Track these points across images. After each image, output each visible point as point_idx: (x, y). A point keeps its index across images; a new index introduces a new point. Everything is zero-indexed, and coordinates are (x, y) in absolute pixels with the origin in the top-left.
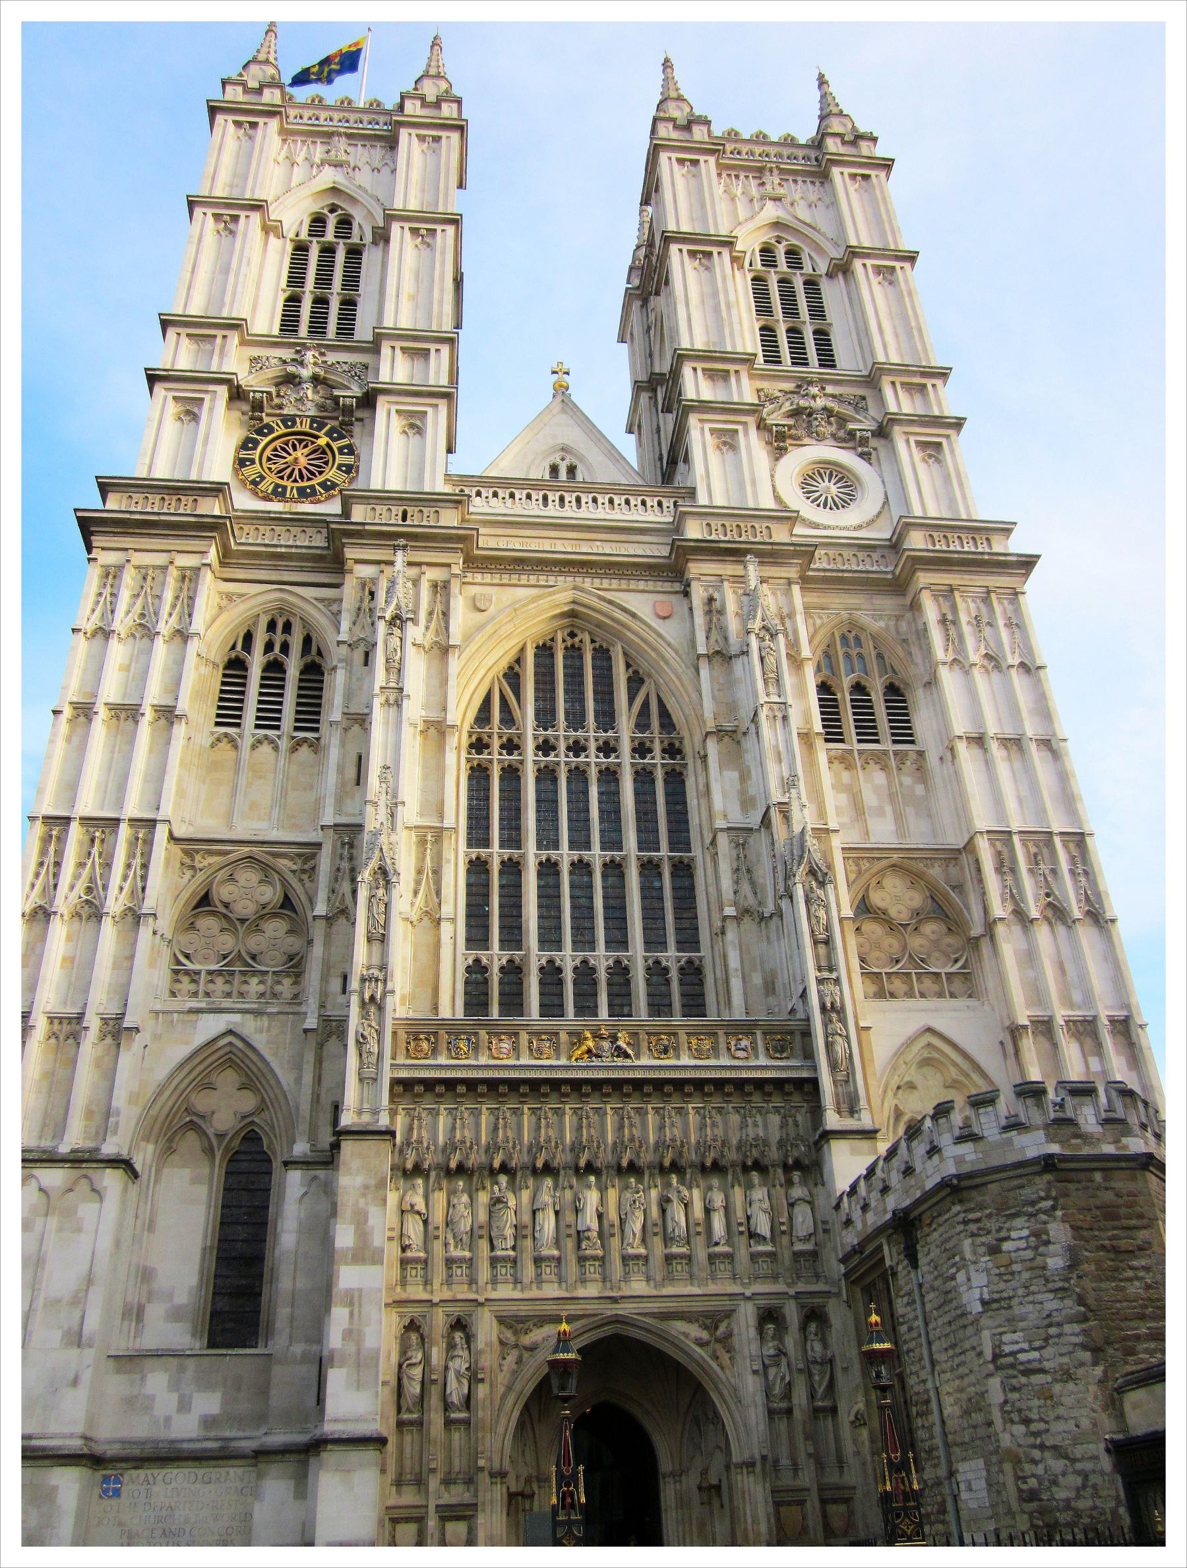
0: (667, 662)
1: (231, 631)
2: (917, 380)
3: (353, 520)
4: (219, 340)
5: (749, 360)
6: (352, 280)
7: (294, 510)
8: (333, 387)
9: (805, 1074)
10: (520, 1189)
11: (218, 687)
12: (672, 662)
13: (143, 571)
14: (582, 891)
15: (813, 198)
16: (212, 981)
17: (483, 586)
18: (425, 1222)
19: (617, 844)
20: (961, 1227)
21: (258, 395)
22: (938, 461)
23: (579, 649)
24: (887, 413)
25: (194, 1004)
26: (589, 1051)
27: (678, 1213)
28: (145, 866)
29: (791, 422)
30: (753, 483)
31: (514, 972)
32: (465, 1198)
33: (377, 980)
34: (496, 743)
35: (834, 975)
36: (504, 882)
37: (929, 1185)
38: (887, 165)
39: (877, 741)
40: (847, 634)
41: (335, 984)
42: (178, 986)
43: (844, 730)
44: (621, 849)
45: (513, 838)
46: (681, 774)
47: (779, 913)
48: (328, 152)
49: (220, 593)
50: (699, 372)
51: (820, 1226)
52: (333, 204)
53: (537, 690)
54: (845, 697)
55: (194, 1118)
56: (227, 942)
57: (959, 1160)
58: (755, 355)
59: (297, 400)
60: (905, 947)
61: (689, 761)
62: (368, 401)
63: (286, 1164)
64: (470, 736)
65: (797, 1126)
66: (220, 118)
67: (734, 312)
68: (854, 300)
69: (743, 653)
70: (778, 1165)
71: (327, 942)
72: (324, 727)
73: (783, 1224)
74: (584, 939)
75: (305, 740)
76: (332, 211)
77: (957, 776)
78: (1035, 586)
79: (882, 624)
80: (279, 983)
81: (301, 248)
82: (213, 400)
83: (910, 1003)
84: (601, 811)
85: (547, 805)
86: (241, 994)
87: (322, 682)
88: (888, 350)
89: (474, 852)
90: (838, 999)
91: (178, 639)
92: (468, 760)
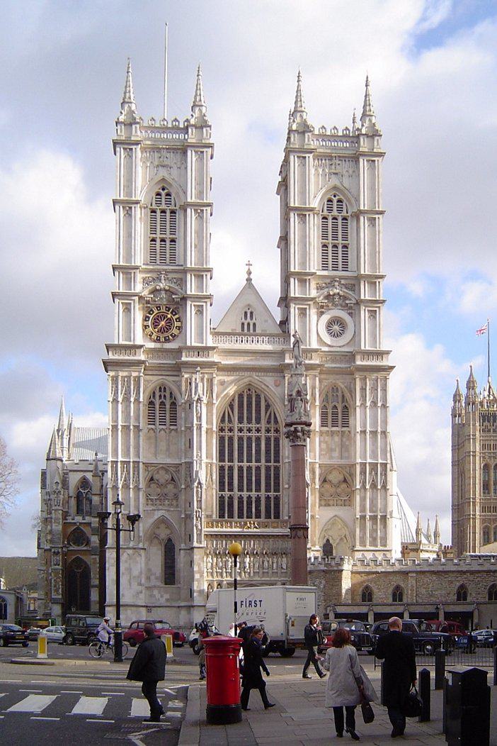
1: (150, 392)
7: (164, 347)
11: (147, 412)
15: (351, 172)
27: (266, 564)
28: (138, 474)
29: (326, 301)
31: (231, 498)
38: (381, 155)
45: (231, 460)
54: (330, 411)
62: (184, 299)
67: (312, 247)
71: (185, 496)
74: (249, 490)
76: (163, 189)
77: (355, 442)
78: (392, 374)
81: (153, 211)
82: (134, 302)
88: (365, 270)
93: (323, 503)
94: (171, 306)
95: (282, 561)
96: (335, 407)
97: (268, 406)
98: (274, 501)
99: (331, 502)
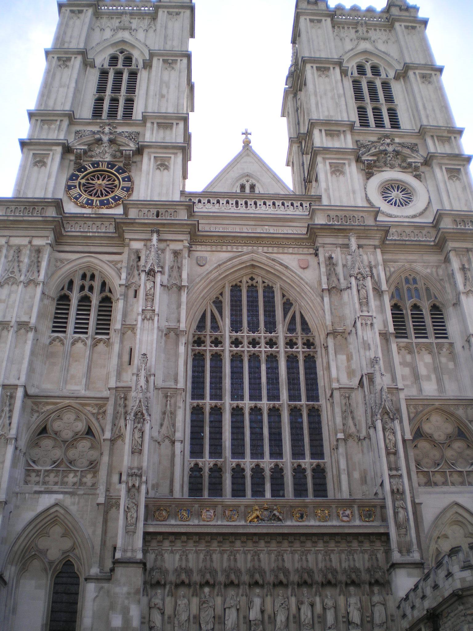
0: (305, 293)
2: (445, 134)
3: (129, 217)
4: (58, 123)
5: (352, 126)
6: (132, 88)
8: (120, 145)
9: (382, 531)
10: (218, 595)
11: (54, 311)
12: (308, 293)
13: (14, 248)
14: (256, 424)
15: (384, 38)
16: (47, 476)
17: (201, 251)
18: (163, 614)
19: (277, 398)
20: (463, 618)
21: (79, 151)
22: (459, 179)
23: (256, 287)
24: (429, 153)
25: (37, 488)
26: (257, 517)
28: (11, 411)
29: (375, 158)
30: (354, 192)
31: (217, 471)
32: (186, 601)
33: (136, 475)
34: (208, 340)
35: (400, 472)
36: (212, 419)
37: (446, 594)
39: (426, 337)
40: (409, 277)
41: (115, 478)
42: (29, 478)
43: (408, 331)
44: (279, 399)
45: (217, 394)
46: (313, 357)
47: (368, 437)
48: (120, 22)
49: (55, 259)
50: (323, 132)
51: (389, 617)
52: (122, 49)
53: (232, 310)
55: (36, 553)
56: (58, 453)
57: (463, 580)
58: (355, 122)
59: (100, 153)
60: (442, 457)
61: (318, 349)
62: (139, 151)
63: (86, 579)
64: (194, 337)
65: (377, 560)
66: (63, 9)
68: (410, 92)
69: (349, 288)
70: (366, 583)
72: (112, 332)
73: (368, 617)
74: (257, 452)
75: (100, 340)
76: (121, 53)
79: (429, 270)
80: (85, 476)
81: (104, 73)
83: (445, 489)
84: (268, 378)
85: (237, 374)
86: (63, 483)
87: (111, 307)
89: (195, 402)
90: (401, 487)
91: (32, 286)
92: (193, 350)
93: (423, 480)
94: (116, 163)
95: (347, 605)
96: (415, 307)
97: (287, 305)
98: (314, 478)
99: (438, 478)
